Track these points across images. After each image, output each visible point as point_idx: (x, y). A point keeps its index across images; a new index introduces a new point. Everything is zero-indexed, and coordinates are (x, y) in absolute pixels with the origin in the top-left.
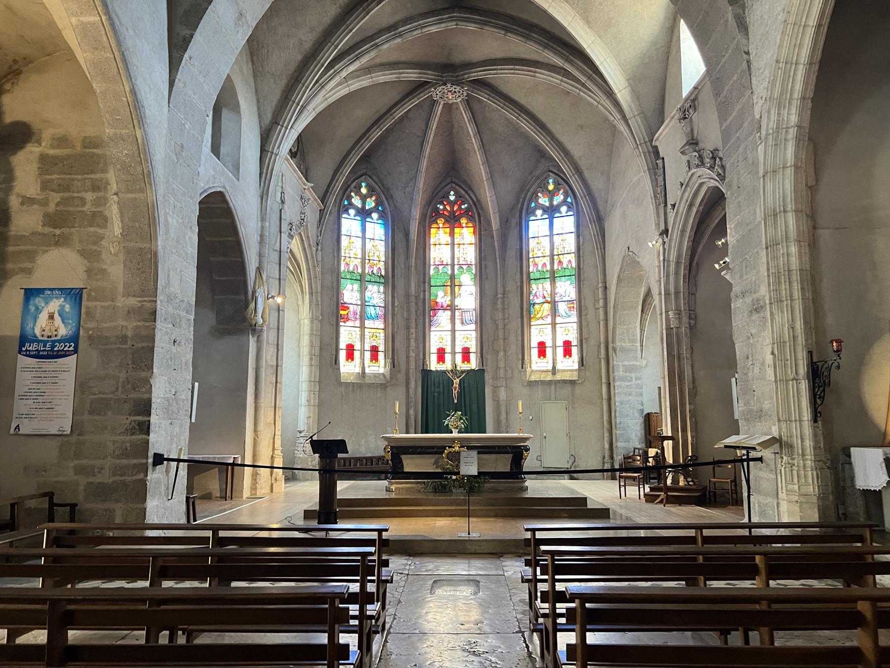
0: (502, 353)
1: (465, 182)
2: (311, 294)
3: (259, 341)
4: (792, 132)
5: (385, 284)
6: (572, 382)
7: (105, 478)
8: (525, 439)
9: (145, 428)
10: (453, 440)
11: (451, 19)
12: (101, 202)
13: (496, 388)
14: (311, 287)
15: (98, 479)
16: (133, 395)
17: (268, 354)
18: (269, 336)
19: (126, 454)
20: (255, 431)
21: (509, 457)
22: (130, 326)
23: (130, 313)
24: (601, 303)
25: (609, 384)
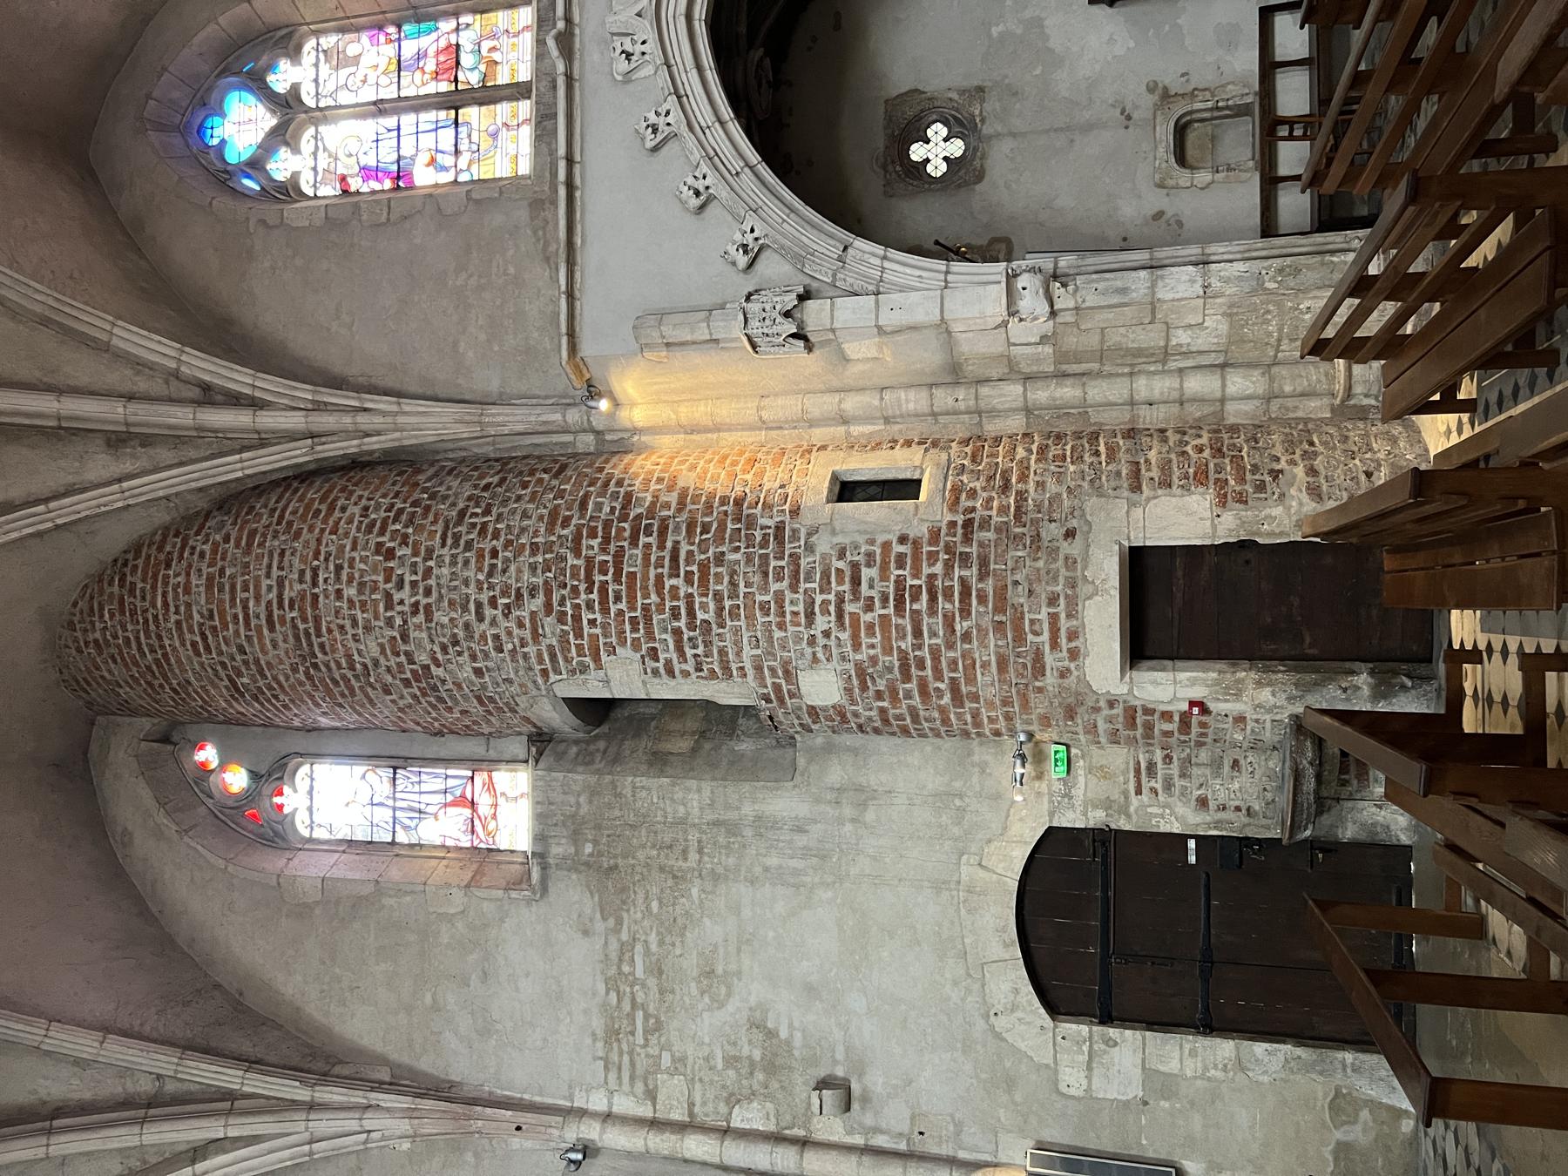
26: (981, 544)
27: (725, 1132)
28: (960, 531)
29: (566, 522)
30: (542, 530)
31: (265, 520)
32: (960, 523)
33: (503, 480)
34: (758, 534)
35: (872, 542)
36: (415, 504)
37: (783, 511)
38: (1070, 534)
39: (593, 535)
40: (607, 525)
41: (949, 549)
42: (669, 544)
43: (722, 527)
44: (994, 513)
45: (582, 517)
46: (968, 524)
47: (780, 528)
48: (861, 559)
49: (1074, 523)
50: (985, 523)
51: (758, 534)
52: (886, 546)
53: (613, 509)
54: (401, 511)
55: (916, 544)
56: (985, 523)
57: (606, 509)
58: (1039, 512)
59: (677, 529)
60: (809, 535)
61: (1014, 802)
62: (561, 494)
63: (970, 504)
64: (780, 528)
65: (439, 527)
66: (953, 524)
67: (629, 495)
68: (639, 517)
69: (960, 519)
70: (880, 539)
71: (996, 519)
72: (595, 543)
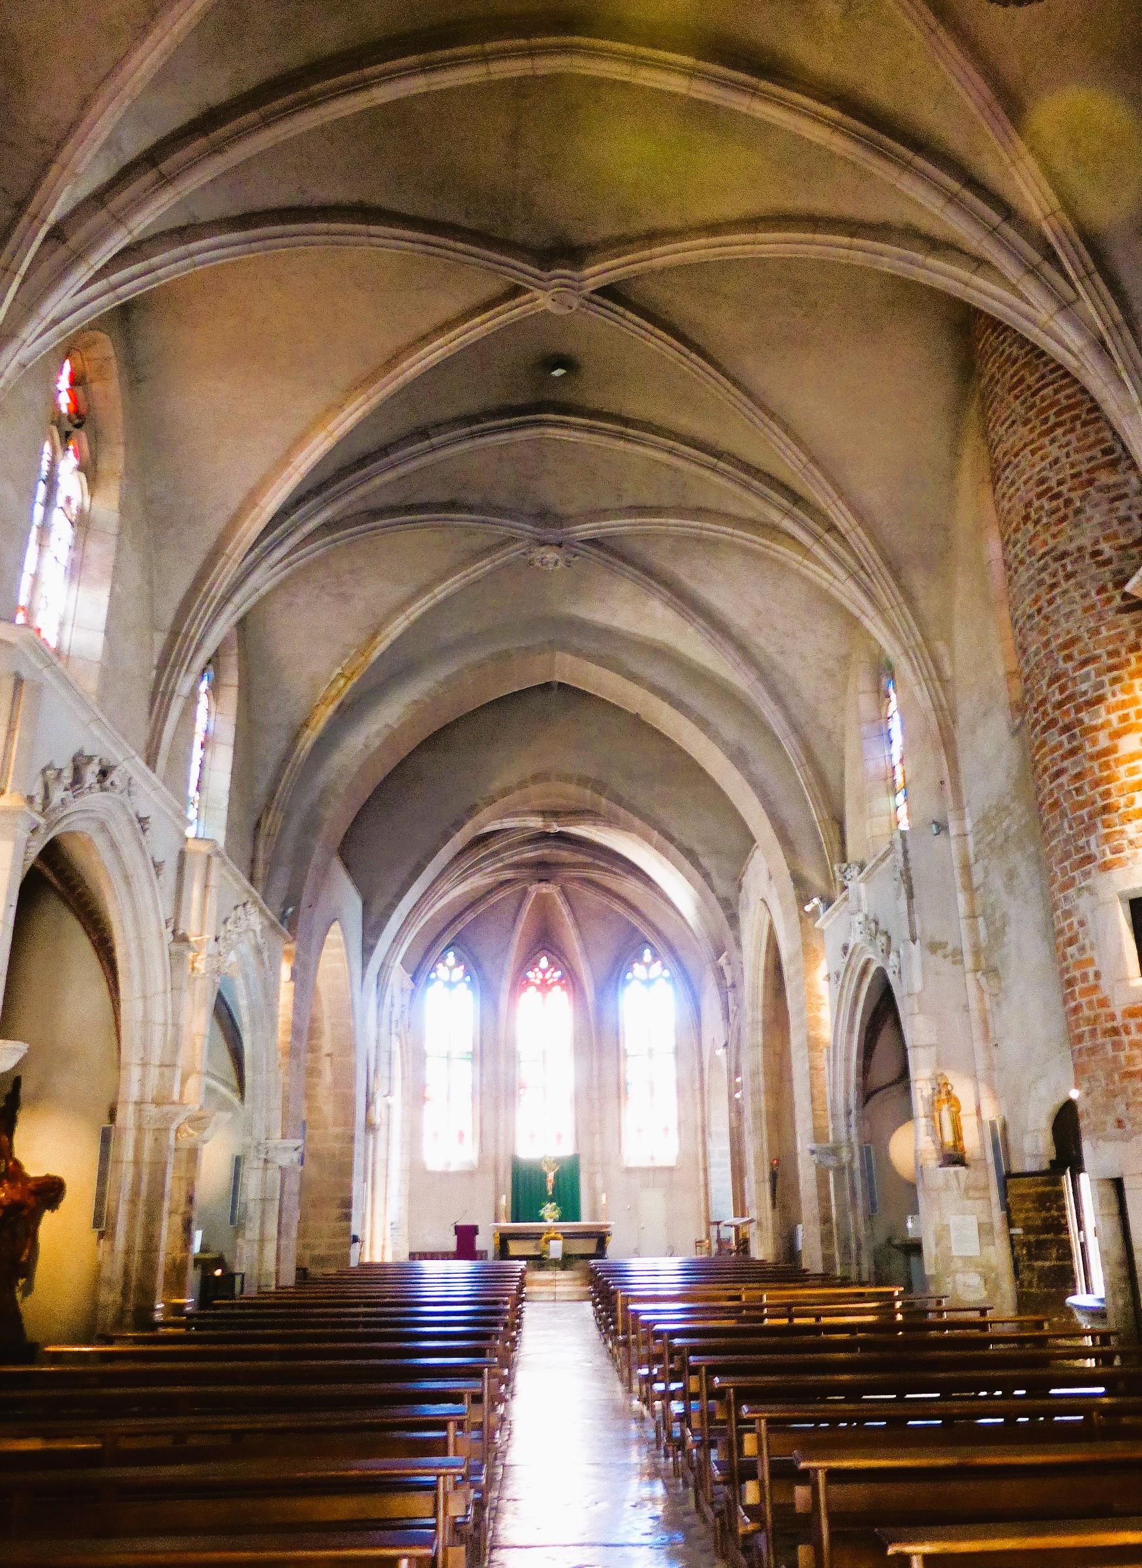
0: (597, 1137)
1: (558, 948)
2: (403, 1078)
3: (375, 1139)
4: (760, 1025)
5: (473, 1060)
6: (671, 1169)
7: (321, 1251)
8: (607, 1227)
9: (347, 1217)
10: (549, 1228)
11: (548, 847)
12: (317, 1060)
13: (592, 1175)
14: (403, 1073)
15: (316, 1252)
16: (341, 1195)
17: (381, 1146)
18: (382, 1133)
19: (334, 1235)
20: (372, 1221)
21: (596, 1240)
22: (336, 1146)
23: (337, 1137)
24: (697, 1085)
25: (705, 1170)
26: (1104, 1045)
27: (973, 916)
28: (1109, 1025)
29: (1069, 658)
30: (1060, 640)
31: (1031, 380)
32: (1115, 1024)
33: (1108, 562)
34: (1081, 842)
35: (1092, 948)
36: (1068, 502)
37: (1104, 855)
38: (1120, 1123)
39: (1062, 689)
40: (1071, 697)
41: (1097, 1017)
42: (1065, 764)
43: (1082, 805)
44: (1127, 1052)
45: (1075, 669)
46: (1115, 1031)
47: (1090, 859)
48: (1081, 942)
49: (1129, 1126)
50: (1117, 1046)
51: (1081, 842)
52: (1091, 962)
53: (1085, 693)
54: (1057, 496)
55: (1096, 988)
56: (1117, 1046)
57: (1084, 687)
58: (1134, 1094)
59: (1075, 764)
60: (1088, 888)
61: (1077, 1086)
62: (1095, 632)
63: (1133, 1029)
64: (1090, 859)
65: (1052, 542)
66: (1112, 1017)
67: (1100, 699)
68: (1081, 722)
69: (1118, 1023)
70: (1095, 954)
71: (1122, 1054)
72: (1058, 697)
